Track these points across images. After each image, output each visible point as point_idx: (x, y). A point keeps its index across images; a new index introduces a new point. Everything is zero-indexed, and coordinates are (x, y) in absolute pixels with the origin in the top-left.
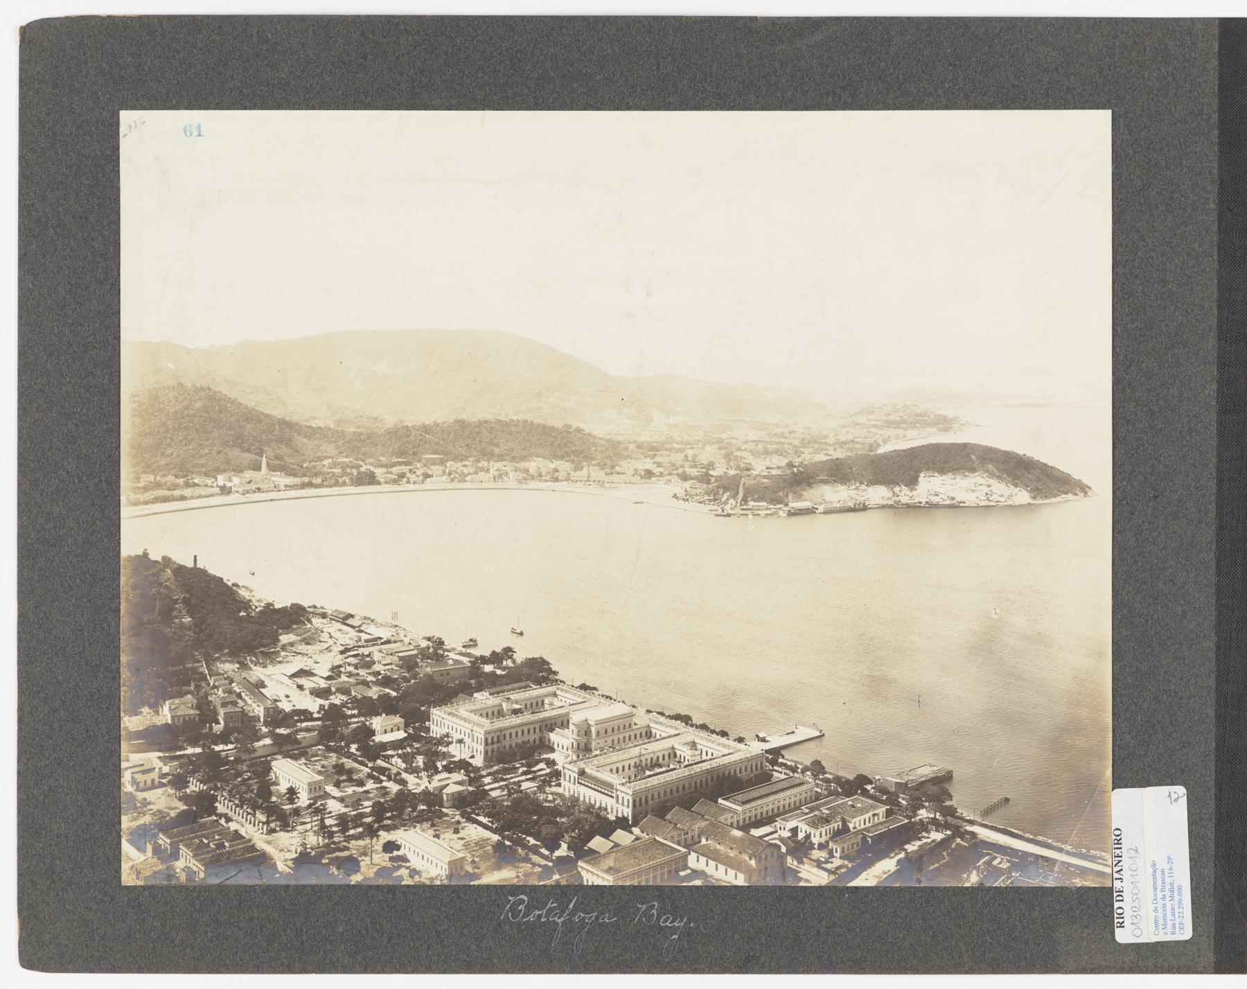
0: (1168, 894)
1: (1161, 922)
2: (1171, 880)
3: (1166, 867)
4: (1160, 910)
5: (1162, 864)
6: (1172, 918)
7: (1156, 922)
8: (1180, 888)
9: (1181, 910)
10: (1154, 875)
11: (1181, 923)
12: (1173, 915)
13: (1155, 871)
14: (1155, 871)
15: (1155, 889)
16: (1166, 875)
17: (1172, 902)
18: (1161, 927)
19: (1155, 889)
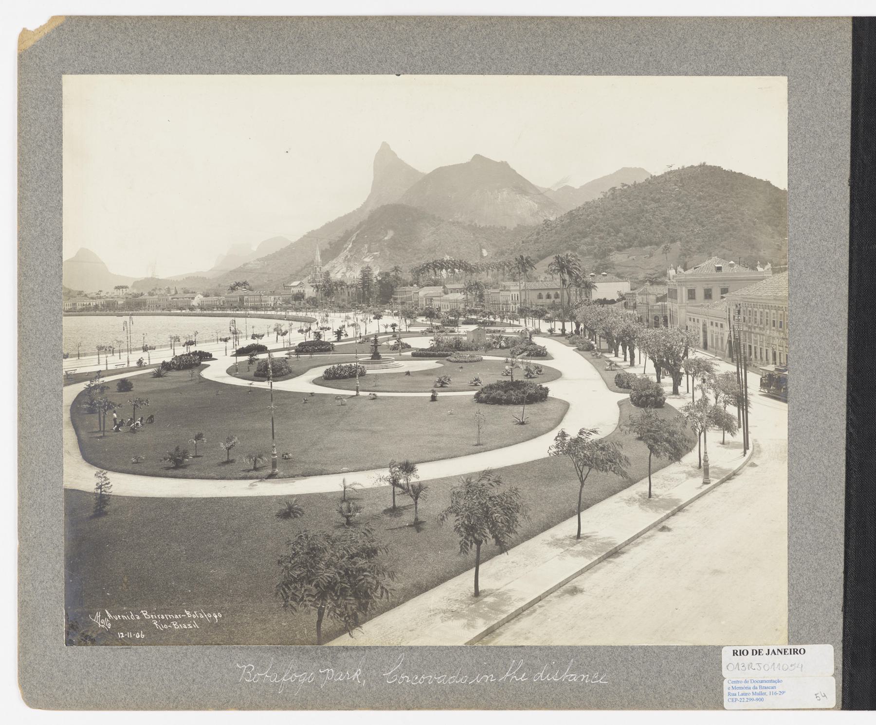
0: (758, 691)
1: (738, 685)
2: (768, 693)
3: (777, 690)
4: (746, 685)
5: (779, 687)
6: (740, 694)
7: (737, 682)
8: (762, 700)
9: (746, 700)
10: (771, 681)
11: (736, 699)
12: (742, 694)
13: (774, 682)
14: (774, 682)
15: (762, 682)
16: (771, 690)
17: (752, 694)
18: (734, 685)
19: (762, 682)
